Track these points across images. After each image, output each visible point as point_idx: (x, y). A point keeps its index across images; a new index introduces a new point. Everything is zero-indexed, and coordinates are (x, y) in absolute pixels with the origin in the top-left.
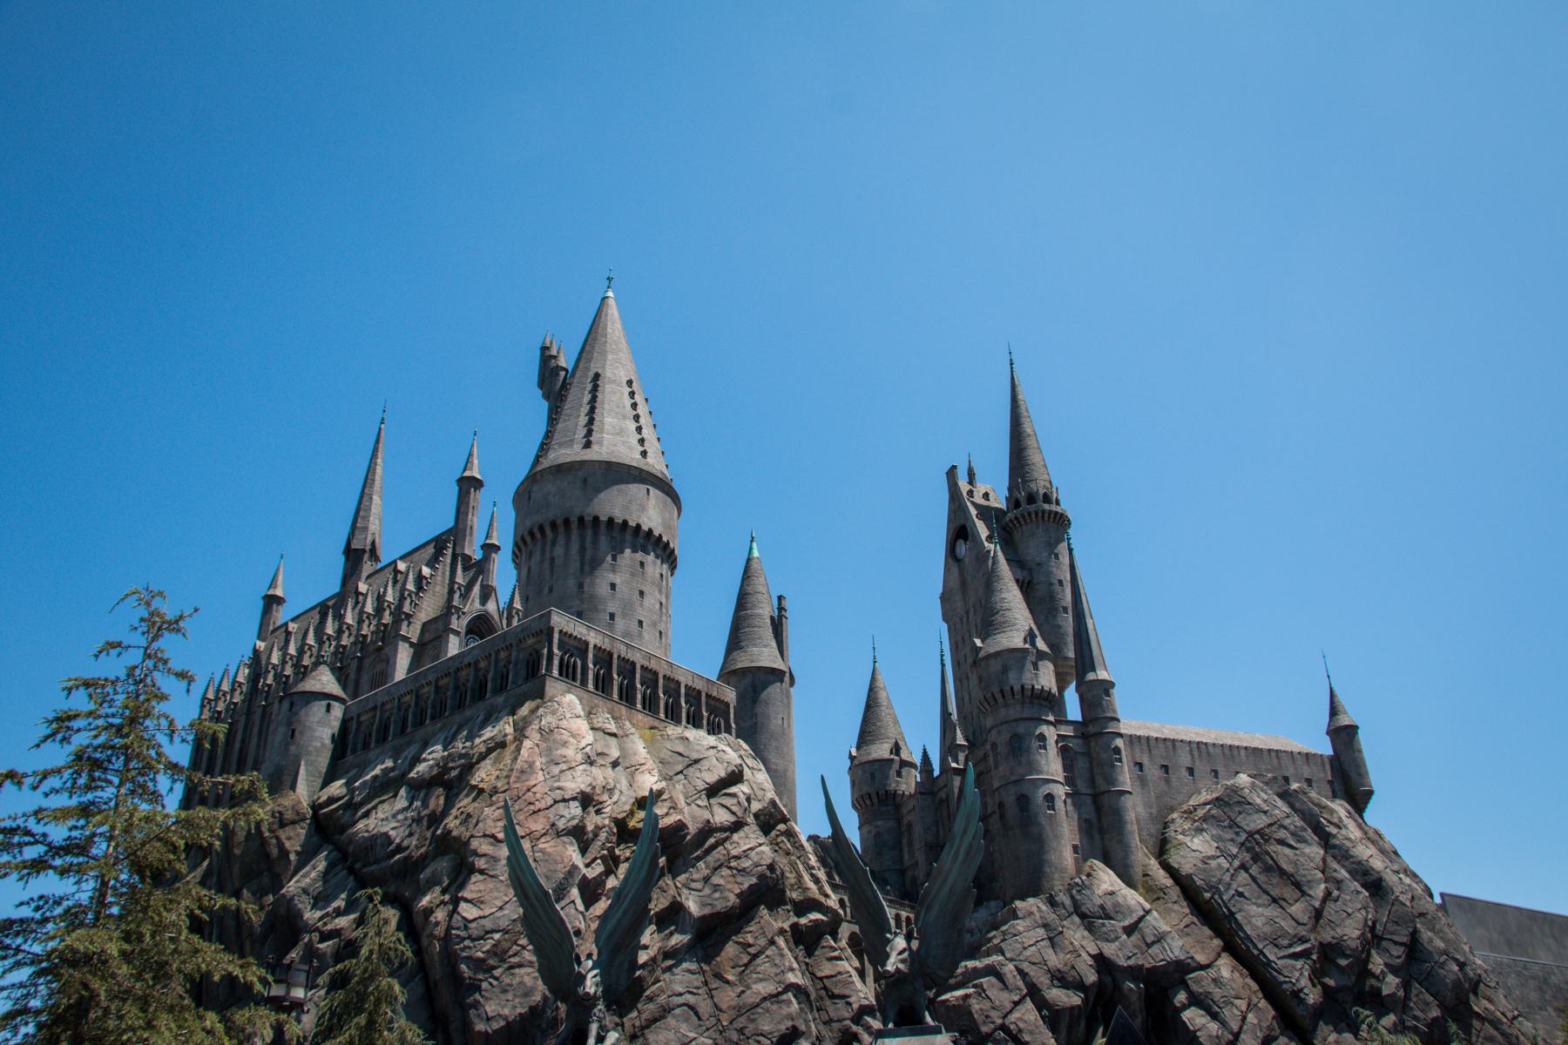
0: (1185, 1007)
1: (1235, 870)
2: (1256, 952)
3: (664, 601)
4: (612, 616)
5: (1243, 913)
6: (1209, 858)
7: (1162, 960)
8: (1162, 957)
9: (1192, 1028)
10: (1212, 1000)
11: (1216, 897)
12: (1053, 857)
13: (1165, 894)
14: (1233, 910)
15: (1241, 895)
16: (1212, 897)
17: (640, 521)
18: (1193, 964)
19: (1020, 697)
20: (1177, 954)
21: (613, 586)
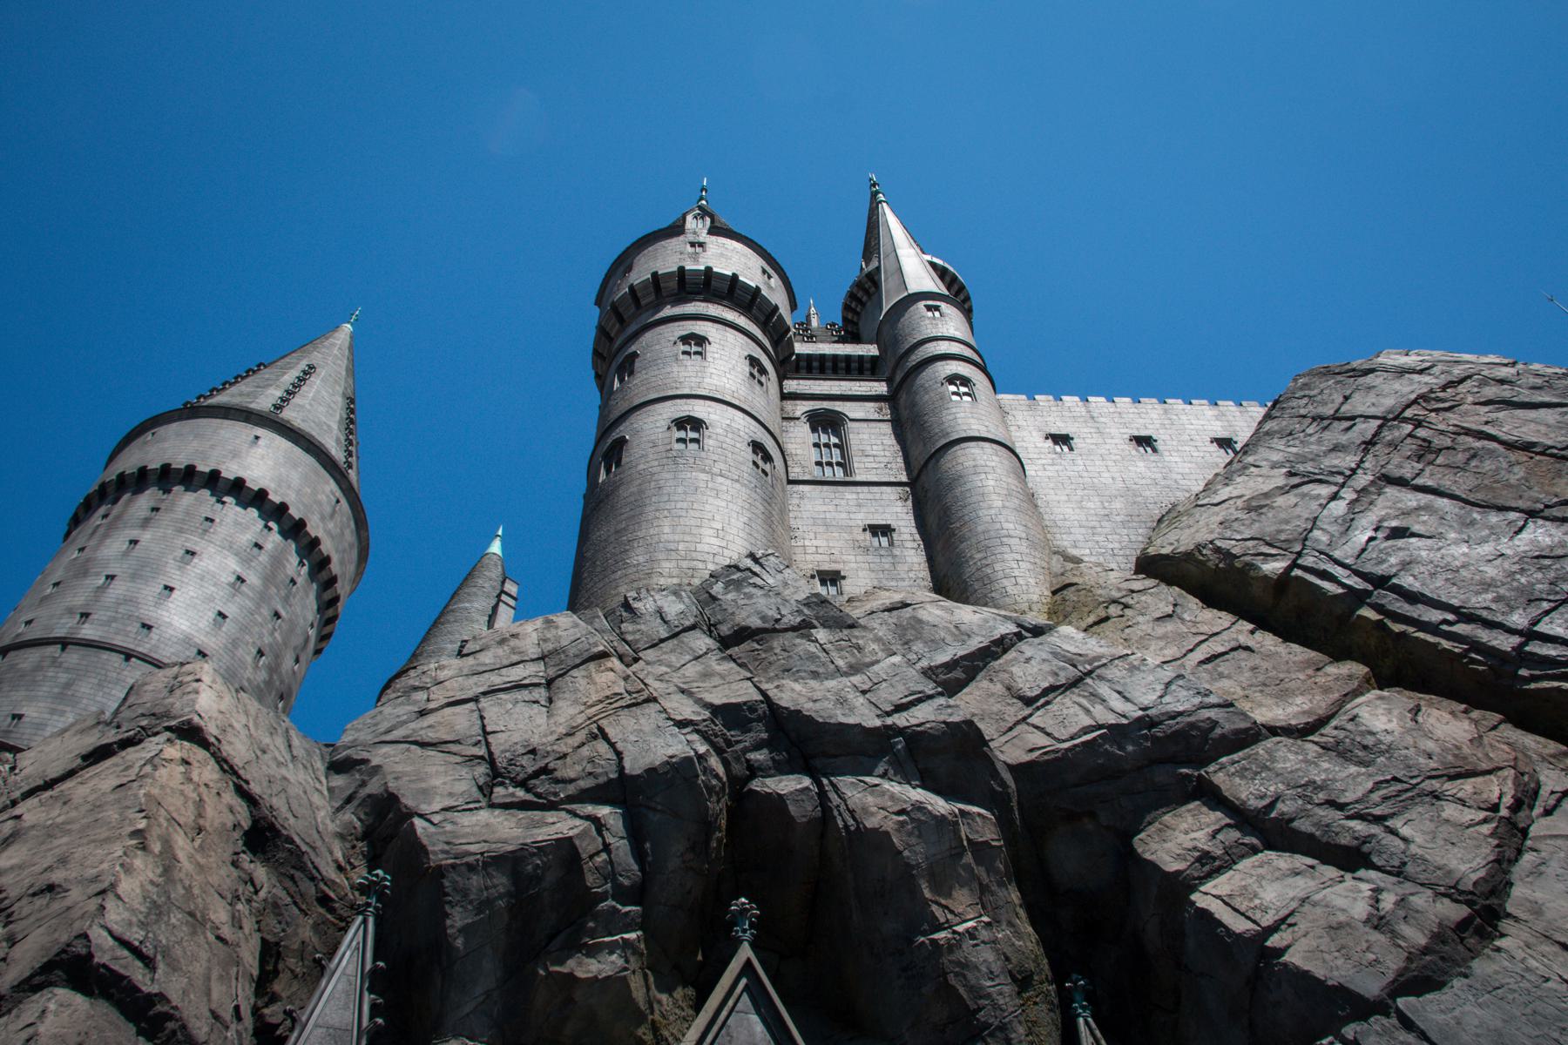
0: (1210, 865)
1: (1363, 491)
2: (1506, 643)
3: (253, 579)
4: (111, 577)
5: (1417, 570)
6: (1266, 495)
7: (1086, 730)
8: (1087, 721)
9: (1239, 925)
10: (1332, 804)
11: (1308, 561)
12: (665, 530)
13: (1126, 606)
14: (1380, 570)
15: (1398, 533)
16: (1294, 565)
17: (222, 468)
18: (1228, 724)
19: (652, 297)
20: (1149, 698)
21: (134, 542)
